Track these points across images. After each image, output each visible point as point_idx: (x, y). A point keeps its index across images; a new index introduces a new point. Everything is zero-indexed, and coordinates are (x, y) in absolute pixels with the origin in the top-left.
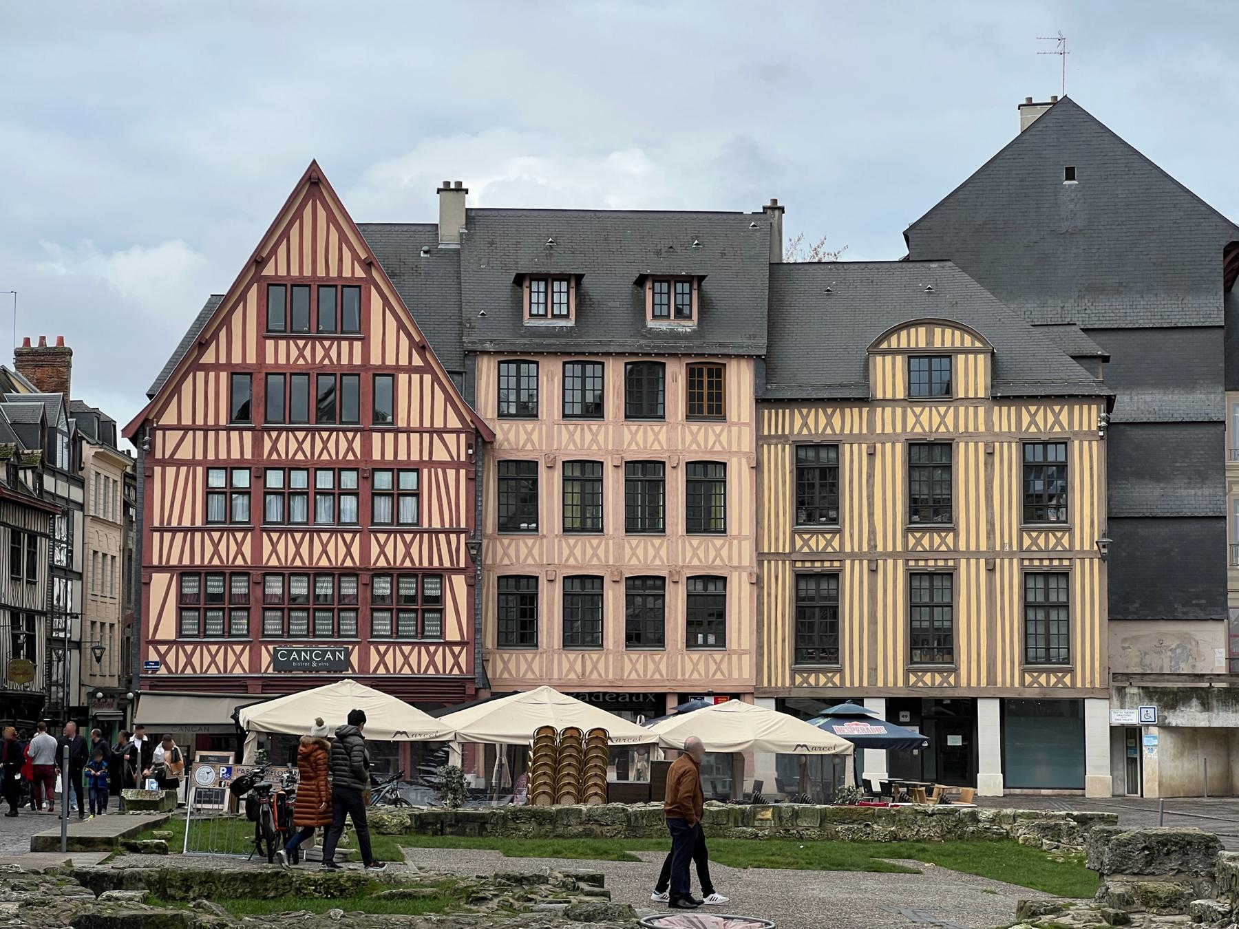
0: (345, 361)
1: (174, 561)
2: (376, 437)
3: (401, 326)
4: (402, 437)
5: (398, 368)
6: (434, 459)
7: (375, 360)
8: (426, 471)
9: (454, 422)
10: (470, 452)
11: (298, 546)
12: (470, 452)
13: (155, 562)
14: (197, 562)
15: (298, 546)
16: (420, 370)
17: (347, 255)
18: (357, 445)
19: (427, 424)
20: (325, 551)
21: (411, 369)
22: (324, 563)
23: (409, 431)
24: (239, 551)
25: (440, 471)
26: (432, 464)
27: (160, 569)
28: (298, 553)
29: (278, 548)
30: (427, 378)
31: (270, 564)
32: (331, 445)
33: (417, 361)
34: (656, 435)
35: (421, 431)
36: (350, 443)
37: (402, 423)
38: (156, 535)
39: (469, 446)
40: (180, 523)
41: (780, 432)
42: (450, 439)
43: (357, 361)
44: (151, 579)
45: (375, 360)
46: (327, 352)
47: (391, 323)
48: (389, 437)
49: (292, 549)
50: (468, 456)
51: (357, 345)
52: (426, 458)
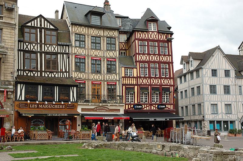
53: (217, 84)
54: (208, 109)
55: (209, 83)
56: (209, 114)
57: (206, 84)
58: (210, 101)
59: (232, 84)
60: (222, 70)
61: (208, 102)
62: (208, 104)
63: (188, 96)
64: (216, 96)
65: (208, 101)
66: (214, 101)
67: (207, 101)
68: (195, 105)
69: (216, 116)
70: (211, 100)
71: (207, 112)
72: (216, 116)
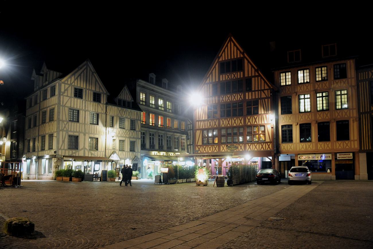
0: (239, 77)
1: (201, 128)
2: (247, 94)
3: (252, 66)
4: (253, 93)
5: (252, 77)
6: (262, 97)
7: (246, 75)
8: (260, 100)
9: (267, 87)
10: (271, 94)
11: (229, 122)
12: (271, 94)
13: (197, 128)
14: (206, 127)
15: (229, 122)
16: (258, 76)
17: (238, 52)
18: (242, 97)
19: (260, 89)
20: (235, 122)
21: (255, 76)
22: (235, 125)
23: (255, 91)
24: (215, 124)
25: (263, 100)
26: (261, 99)
27: (198, 130)
28: (229, 123)
29: (222, 123)
30: (259, 78)
31: (222, 126)
32: (236, 97)
33: (257, 74)
34: (325, 85)
35: (258, 91)
36: (240, 96)
37: (253, 89)
38: (197, 123)
39: (271, 93)
40: (202, 119)
41: (362, 79)
42: (266, 92)
43: (242, 76)
44: (196, 132)
45: (246, 75)
46: (234, 76)
47: (250, 66)
48: (250, 93)
49: (227, 122)
50: (270, 95)
51: (242, 73)
52: (260, 97)
53: (81, 108)
54: (63, 141)
55: (68, 105)
56: (64, 149)
57: (64, 106)
58: (67, 131)
59: (102, 112)
60: (90, 92)
61: (64, 133)
62: (64, 135)
63: (37, 124)
64: (78, 124)
65: (65, 131)
66: (74, 132)
67: (63, 130)
68: (45, 136)
69: (75, 153)
70: (70, 130)
71: (62, 146)
72: (75, 153)
